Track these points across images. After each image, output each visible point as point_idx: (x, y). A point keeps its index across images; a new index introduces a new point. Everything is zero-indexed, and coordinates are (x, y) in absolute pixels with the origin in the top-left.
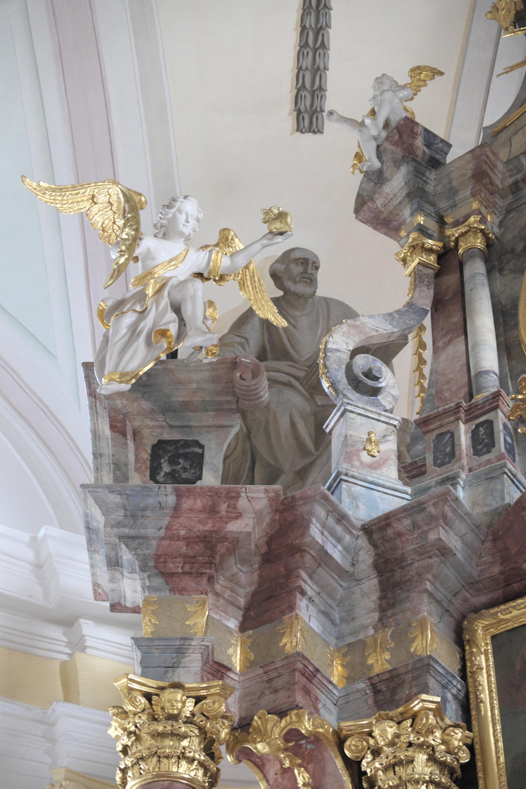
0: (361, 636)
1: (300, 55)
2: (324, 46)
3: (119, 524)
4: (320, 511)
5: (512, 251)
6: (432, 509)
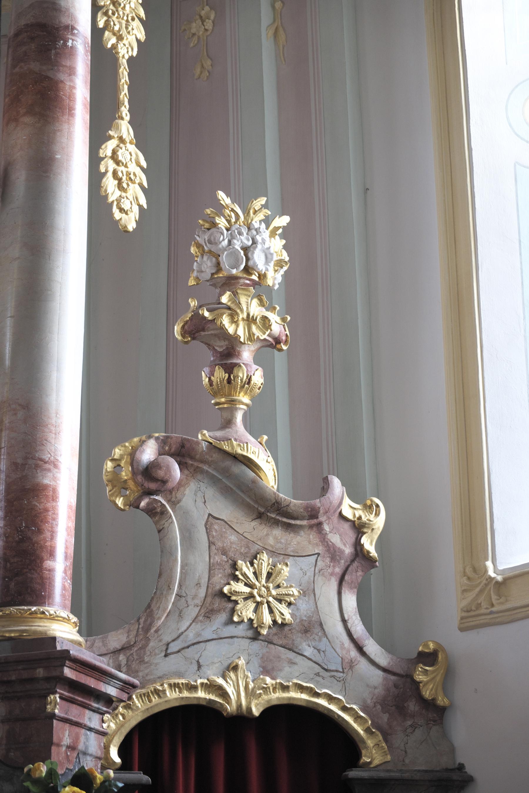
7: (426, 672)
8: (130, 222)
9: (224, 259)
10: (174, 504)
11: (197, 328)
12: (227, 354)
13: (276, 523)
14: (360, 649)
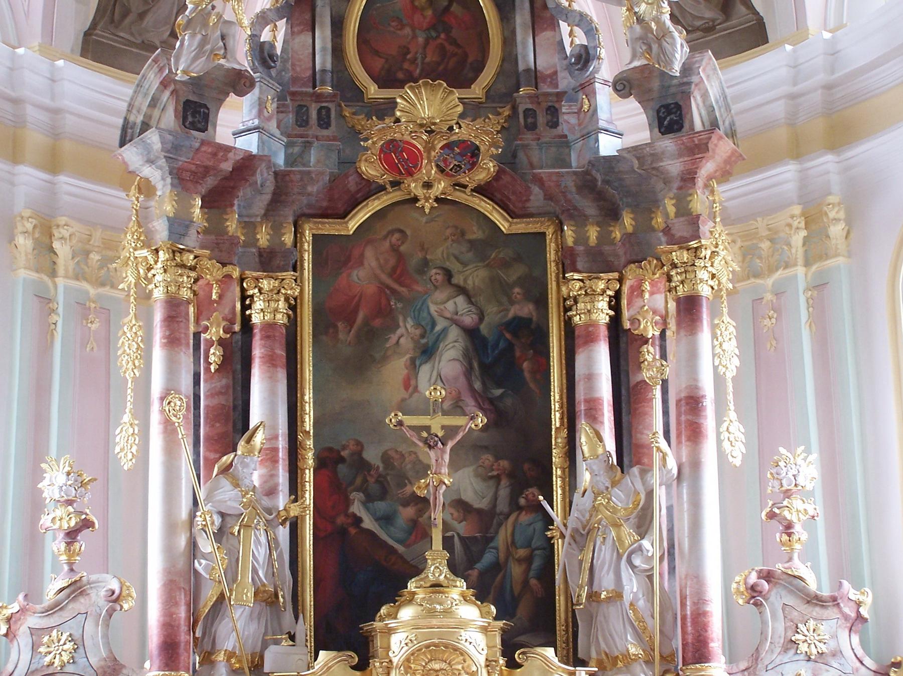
0: (253, 220)
3: (168, 151)
7: (895, 672)
8: (738, 462)
9: (784, 482)
10: (766, 600)
11: (772, 516)
12: (788, 528)
13: (817, 605)
14: (861, 662)
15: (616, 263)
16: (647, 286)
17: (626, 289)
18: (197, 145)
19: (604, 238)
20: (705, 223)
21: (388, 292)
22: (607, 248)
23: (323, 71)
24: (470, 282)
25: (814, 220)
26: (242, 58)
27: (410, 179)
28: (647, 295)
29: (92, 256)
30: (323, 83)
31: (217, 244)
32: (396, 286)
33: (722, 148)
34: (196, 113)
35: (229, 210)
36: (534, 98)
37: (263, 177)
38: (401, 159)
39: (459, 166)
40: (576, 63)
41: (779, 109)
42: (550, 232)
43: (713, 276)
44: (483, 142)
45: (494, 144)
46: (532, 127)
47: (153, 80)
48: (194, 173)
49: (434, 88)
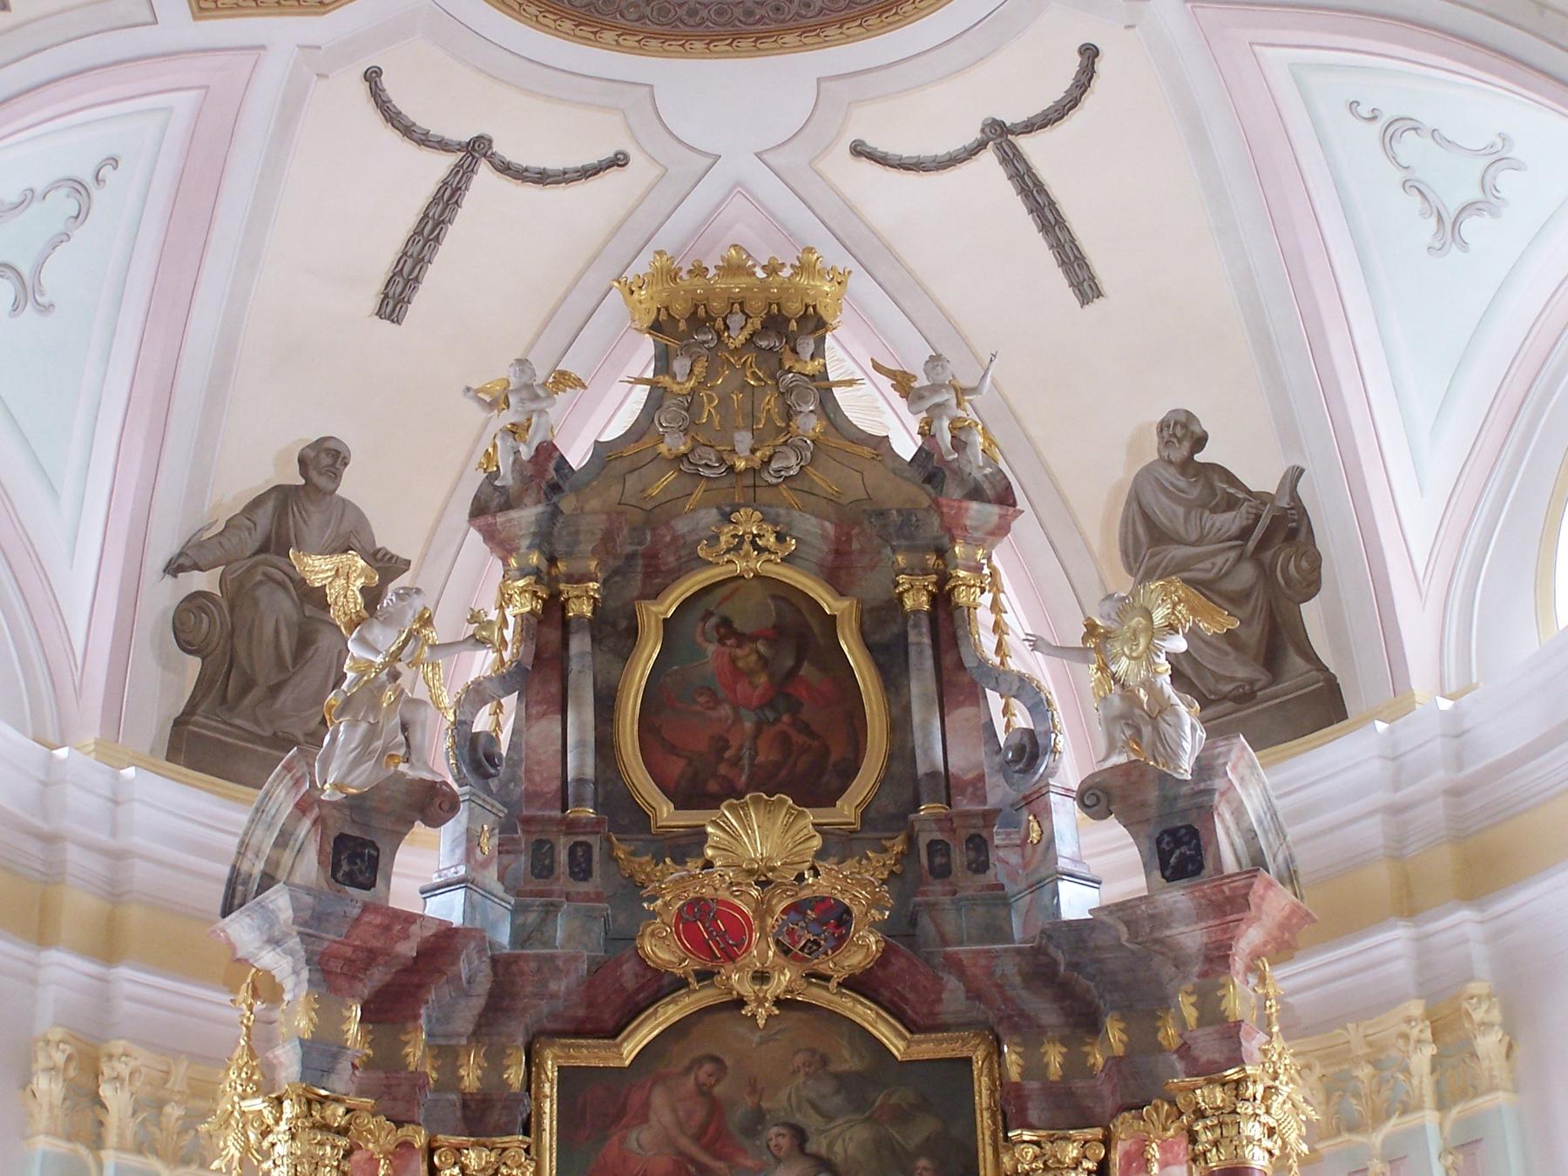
0: (453, 1042)
1: (411, 240)
2: (437, 240)
3: (305, 924)
4: (472, 945)
5: (614, 625)
6: (560, 963)
15: (1098, 1110)
16: (1154, 1151)
17: (1116, 1157)
18: (356, 912)
19: (1075, 1065)
20: (1251, 1037)
21: (692, 1169)
22: (1079, 1084)
23: (580, 781)
24: (838, 1148)
25: (1447, 1025)
26: (438, 761)
27: (730, 966)
28: (1155, 1169)
29: (168, 1109)
30: (580, 801)
31: (389, 1086)
32: (705, 1159)
33: (1274, 902)
34: (356, 856)
35: (410, 1026)
36: (943, 822)
37: (471, 966)
38: (713, 931)
39: (815, 942)
40: (1015, 761)
41: (1372, 832)
42: (978, 1057)
43: (1271, 1132)
44: (857, 900)
45: (875, 903)
46: (943, 872)
47: (282, 799)
48: (349, 962)
49: (771, 808)
